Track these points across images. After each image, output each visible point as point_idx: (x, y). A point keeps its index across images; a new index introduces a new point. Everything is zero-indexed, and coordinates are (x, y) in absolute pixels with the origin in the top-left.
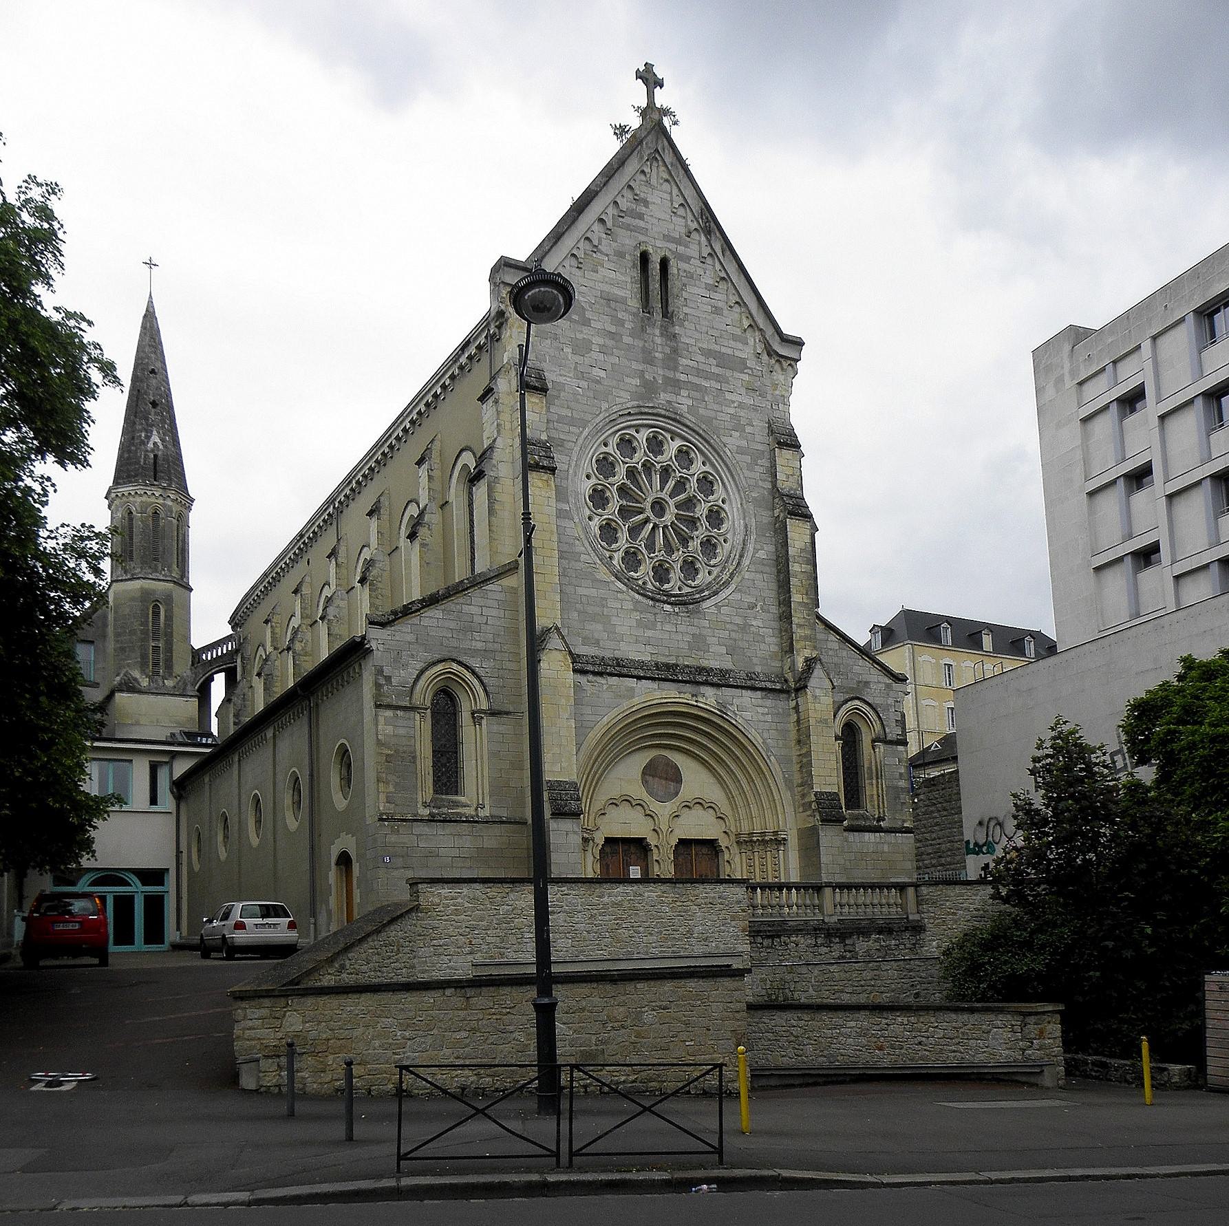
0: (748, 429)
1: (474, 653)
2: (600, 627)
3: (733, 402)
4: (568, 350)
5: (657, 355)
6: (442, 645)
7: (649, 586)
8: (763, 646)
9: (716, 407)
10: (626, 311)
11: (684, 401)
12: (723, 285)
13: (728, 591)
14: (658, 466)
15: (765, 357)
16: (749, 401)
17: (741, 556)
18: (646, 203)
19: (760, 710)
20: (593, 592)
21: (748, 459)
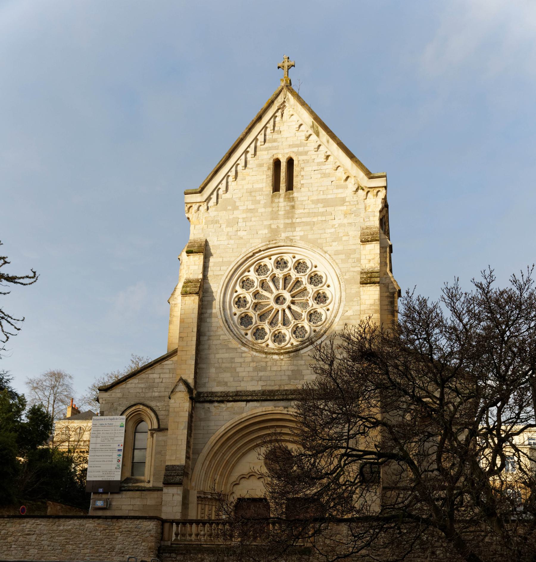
1: (154, 398)
2: (229, 375)
6: (136, 396)
16: (346, 221)
17: (335, 317)
21: (343, 256)
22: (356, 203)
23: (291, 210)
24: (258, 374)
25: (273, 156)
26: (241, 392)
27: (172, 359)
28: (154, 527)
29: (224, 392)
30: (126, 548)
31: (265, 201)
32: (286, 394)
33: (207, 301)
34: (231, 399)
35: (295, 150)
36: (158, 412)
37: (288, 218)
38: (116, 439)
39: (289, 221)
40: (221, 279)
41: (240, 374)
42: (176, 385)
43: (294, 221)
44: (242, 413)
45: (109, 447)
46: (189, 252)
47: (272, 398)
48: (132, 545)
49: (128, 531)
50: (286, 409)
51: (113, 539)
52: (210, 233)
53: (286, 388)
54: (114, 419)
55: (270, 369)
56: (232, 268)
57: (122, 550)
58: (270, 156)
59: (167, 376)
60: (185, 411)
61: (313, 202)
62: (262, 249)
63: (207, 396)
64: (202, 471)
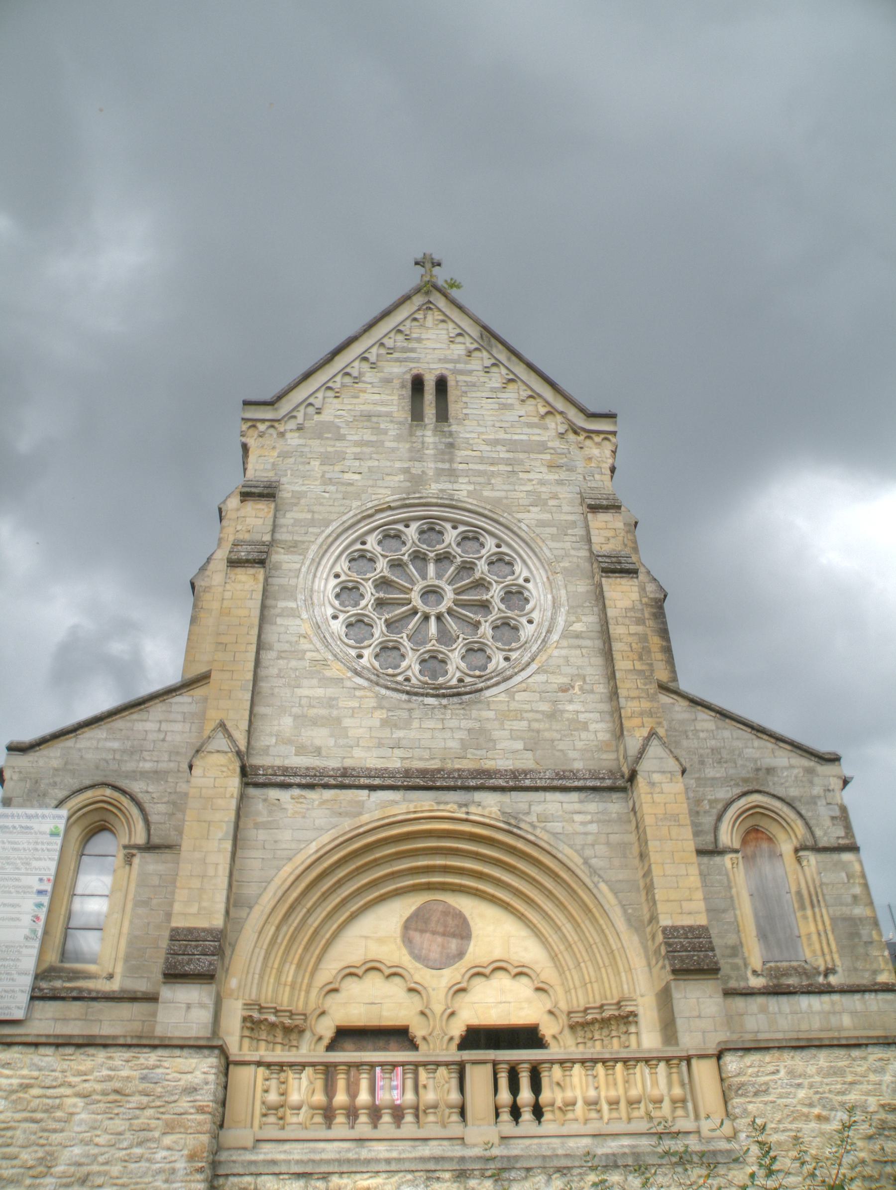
0: (551, 502)
1: (143, 775)
3: (532, 480)
4: (315, 464)
5: (427, 452)
7: (414, 681)
8: (584, 735)
9: (506, 487)
10: (392, 421)
11: (463, 487)
12: (512, 387)
13: (524, 674)
14: (432, 555)
15: (571, 436)
16: (552, 477)
17: (549, 631)
18: (419, 340)
19: (578, 818)
20: (320, 692)
21: (554, 530)
22: (566, 451)
23: (448, 450)
24: (392, 734)
25: (411, 370)
26: (354, 769)
27: (191, 692)
28: (212, 1078)
29: (313, 768)
30: (101, 1159)
31: (398, 432)
32: (460, 777)
33: (279, 585)
34: (332, 782)
35: (450, 366)
36: (148, 807)
37: (443, 461)
38: (35, 864)
39: (446, 466)
40: (308, 549)
41: (351, 733)
42: (209, 737)
43: (455, 466)
44: (360, 814)
45: (17, 883)
46: (246, 496)
47: (430, 783)
48: (125, 1144)
49: (117, 1092)
50: (464, 809)
51: (54, 1125)
52: (289, 472)
53: (457, 766)
54: (37, 816)
55: (418, 726)
56: (332, 532)
57: (85, 1169)
58: (404, 370)
59: (178, 727)
60: (228, 796)
61: (487, 442)
62: (392, 505)
63: (275, 775)
64: (257, 950)
